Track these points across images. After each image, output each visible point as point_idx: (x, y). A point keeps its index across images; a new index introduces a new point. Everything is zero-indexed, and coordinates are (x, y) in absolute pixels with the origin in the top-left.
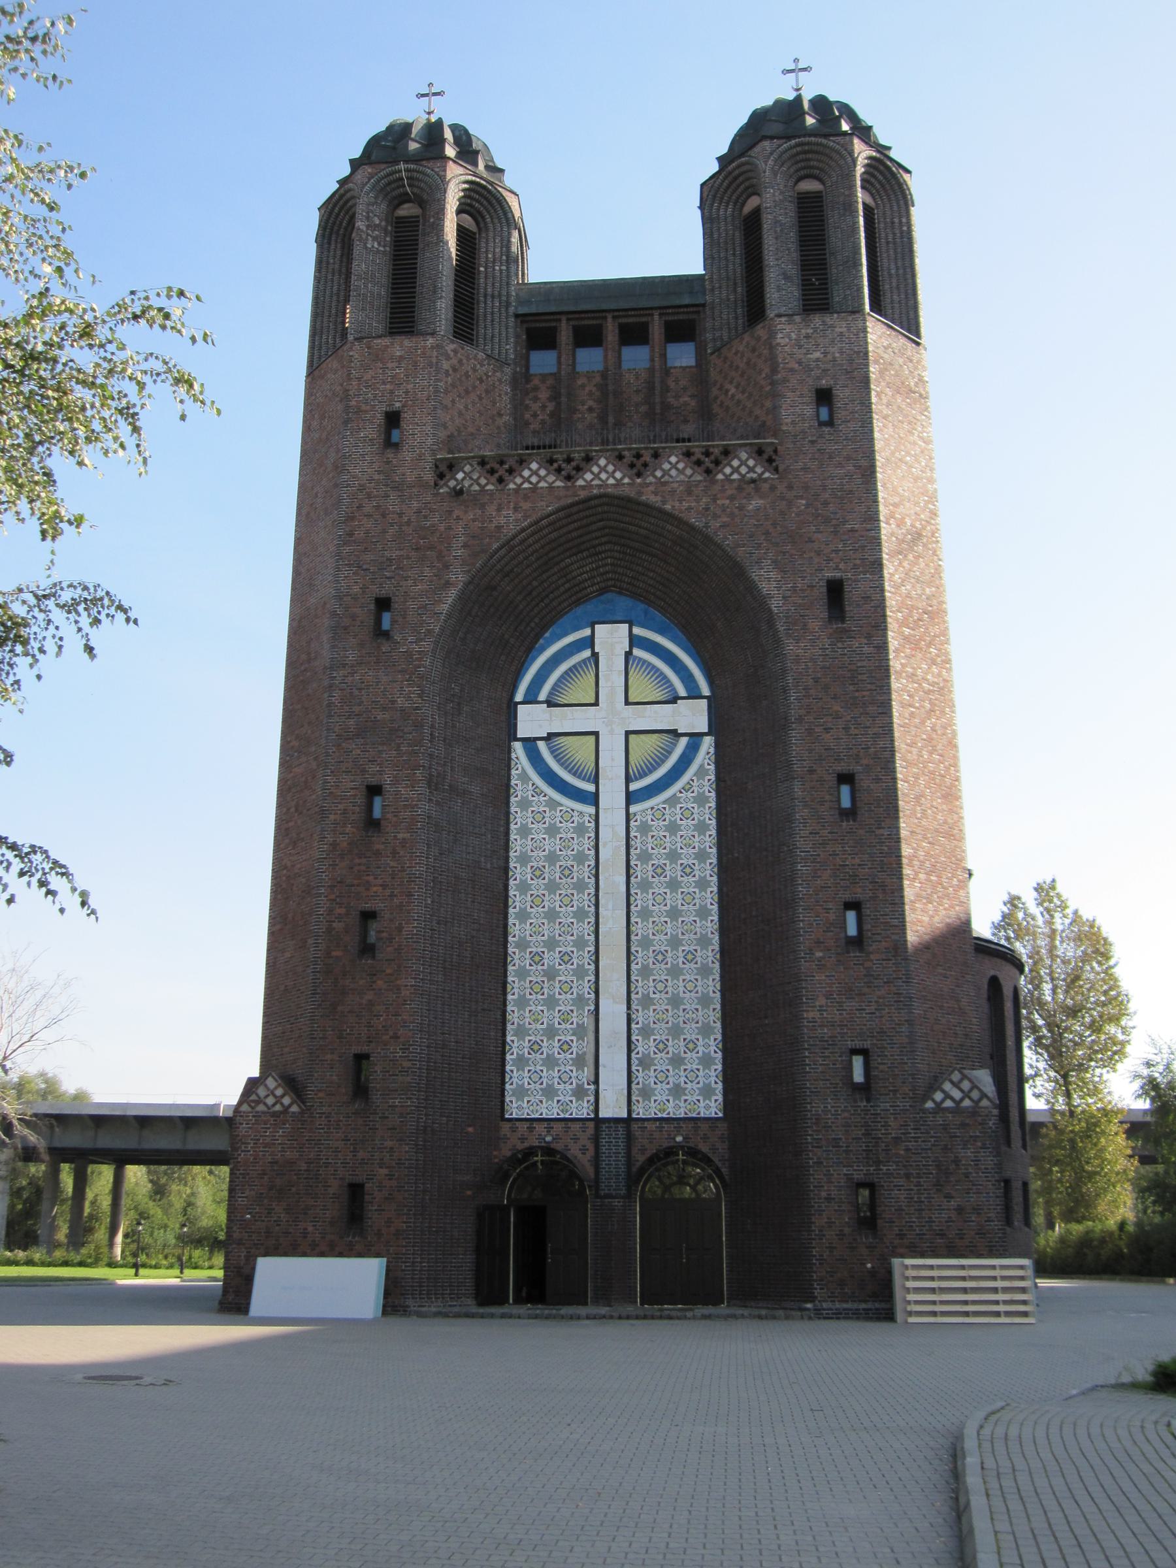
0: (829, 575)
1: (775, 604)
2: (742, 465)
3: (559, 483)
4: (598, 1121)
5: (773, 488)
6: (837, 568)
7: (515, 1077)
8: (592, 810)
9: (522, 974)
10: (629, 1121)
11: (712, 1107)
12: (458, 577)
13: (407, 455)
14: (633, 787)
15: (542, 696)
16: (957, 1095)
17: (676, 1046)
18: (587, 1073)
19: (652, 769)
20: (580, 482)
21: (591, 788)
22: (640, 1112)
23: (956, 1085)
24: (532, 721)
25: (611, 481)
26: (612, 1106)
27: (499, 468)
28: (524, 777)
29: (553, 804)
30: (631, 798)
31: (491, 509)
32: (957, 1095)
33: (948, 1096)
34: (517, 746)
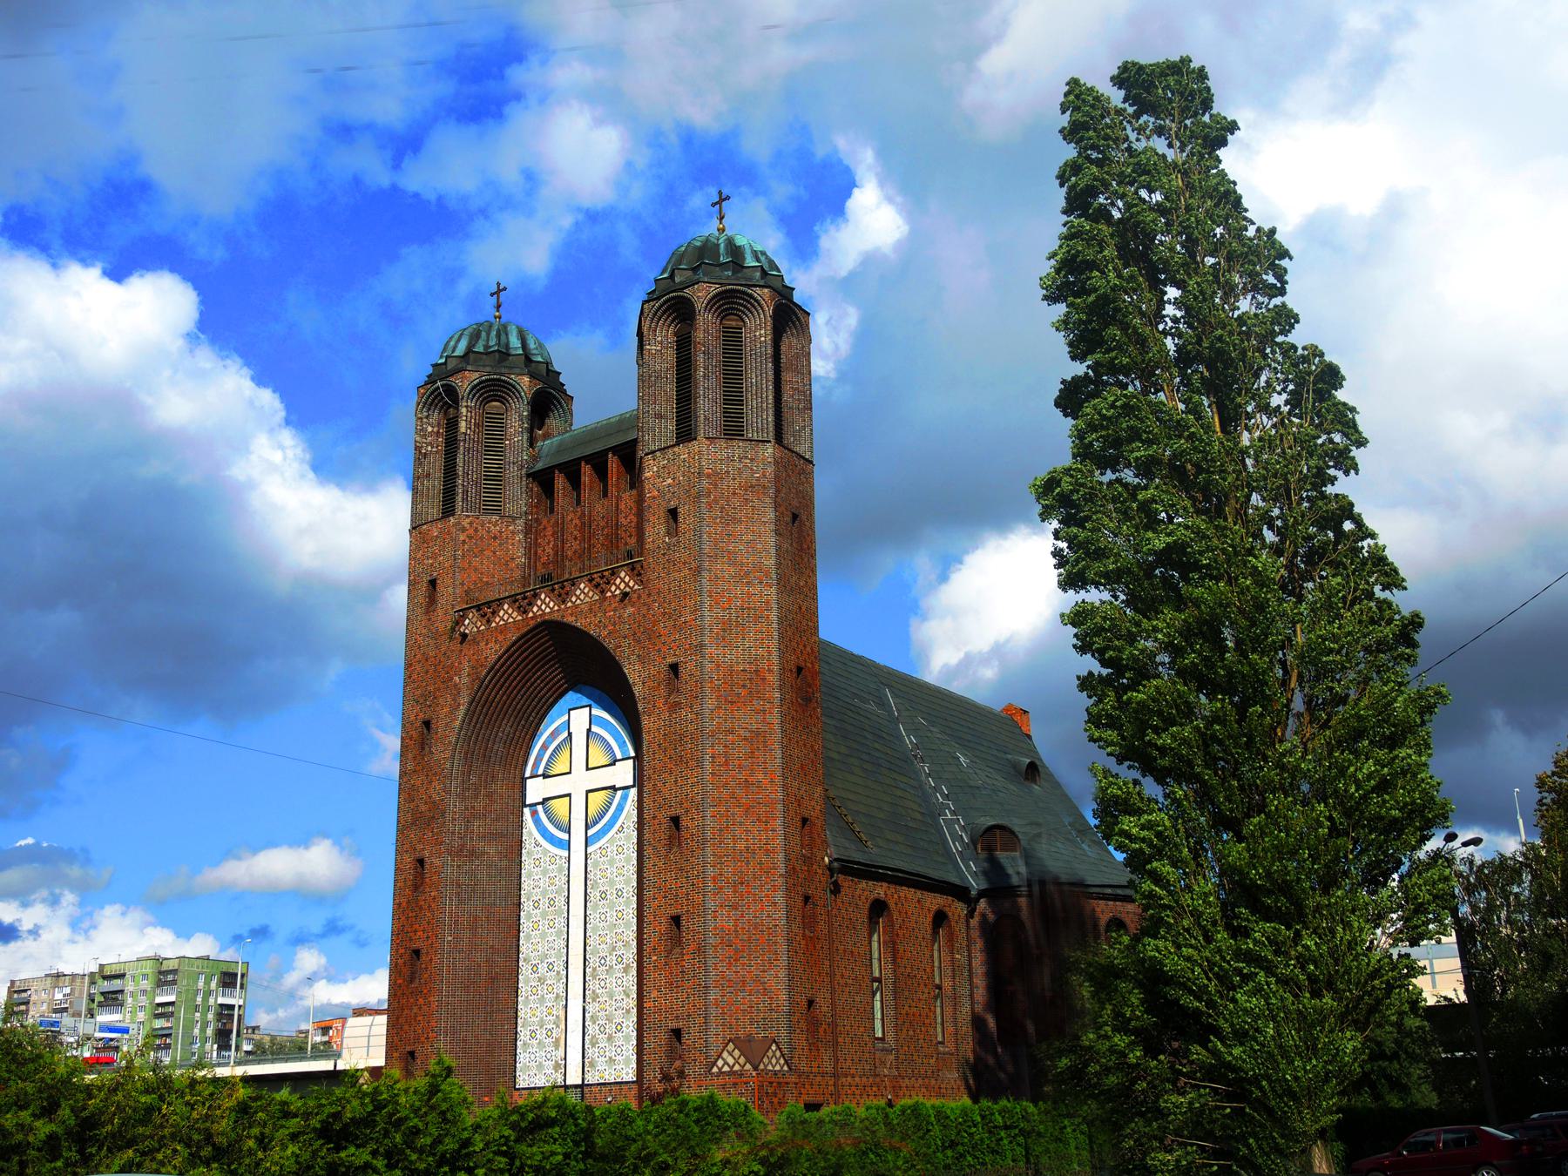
0: (670, 660)
1: (637, 690)
2: (624, 581)
4: (566, 1087)
5: (639, 597)
7: (523, 1058)
8: (565, 854)
9: (527, 981)
10: (582, 1086)
11: (629, 1074)
12: (464, 700)
15: (540, 772)
16: (731, 1061)
17: (611, 1028)
18: (561, 1053)
19: (601, 817)
21: (565, 836)
22: (590, 1079)
23: (730, 1054)
24: (535, 790)
26: (574, 1078)
28: (530, 833)
29: (546, 851)
31: (482, 644)
32: (731, 1061)
33: (726, 1063)
34: (527, 811)
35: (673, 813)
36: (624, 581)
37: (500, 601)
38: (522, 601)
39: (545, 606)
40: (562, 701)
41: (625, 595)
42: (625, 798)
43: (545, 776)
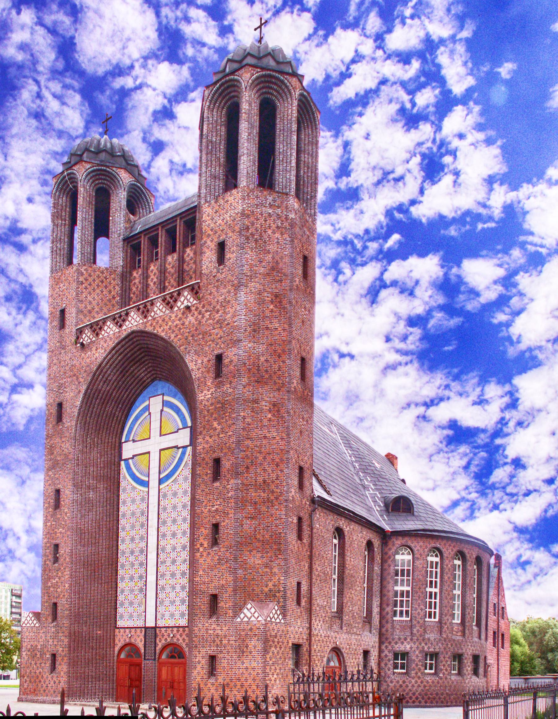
0: (216, 352)
3: (117, 330)
6: (220, 348)
13: (67, 330)
14: (162, 476)
20: (124, 327)
25: (136, 323)
27: (96, 328)
30: (161, 481)
34: (123, 463)
35: (215, 456)
36: (187, 299)
37: (104, 321)
38: (119, 320)
39: (135, 321)
40: (145, 392)
41: (188, 308)
42: (183, 454)
43: (134, 441)
